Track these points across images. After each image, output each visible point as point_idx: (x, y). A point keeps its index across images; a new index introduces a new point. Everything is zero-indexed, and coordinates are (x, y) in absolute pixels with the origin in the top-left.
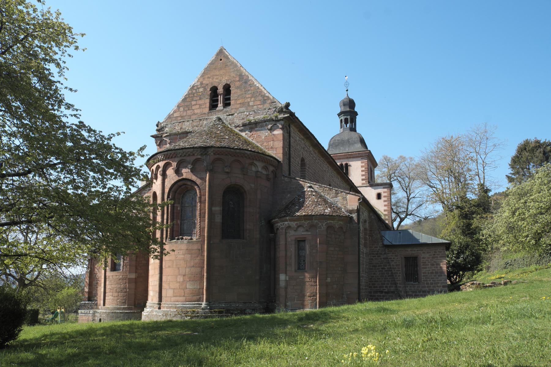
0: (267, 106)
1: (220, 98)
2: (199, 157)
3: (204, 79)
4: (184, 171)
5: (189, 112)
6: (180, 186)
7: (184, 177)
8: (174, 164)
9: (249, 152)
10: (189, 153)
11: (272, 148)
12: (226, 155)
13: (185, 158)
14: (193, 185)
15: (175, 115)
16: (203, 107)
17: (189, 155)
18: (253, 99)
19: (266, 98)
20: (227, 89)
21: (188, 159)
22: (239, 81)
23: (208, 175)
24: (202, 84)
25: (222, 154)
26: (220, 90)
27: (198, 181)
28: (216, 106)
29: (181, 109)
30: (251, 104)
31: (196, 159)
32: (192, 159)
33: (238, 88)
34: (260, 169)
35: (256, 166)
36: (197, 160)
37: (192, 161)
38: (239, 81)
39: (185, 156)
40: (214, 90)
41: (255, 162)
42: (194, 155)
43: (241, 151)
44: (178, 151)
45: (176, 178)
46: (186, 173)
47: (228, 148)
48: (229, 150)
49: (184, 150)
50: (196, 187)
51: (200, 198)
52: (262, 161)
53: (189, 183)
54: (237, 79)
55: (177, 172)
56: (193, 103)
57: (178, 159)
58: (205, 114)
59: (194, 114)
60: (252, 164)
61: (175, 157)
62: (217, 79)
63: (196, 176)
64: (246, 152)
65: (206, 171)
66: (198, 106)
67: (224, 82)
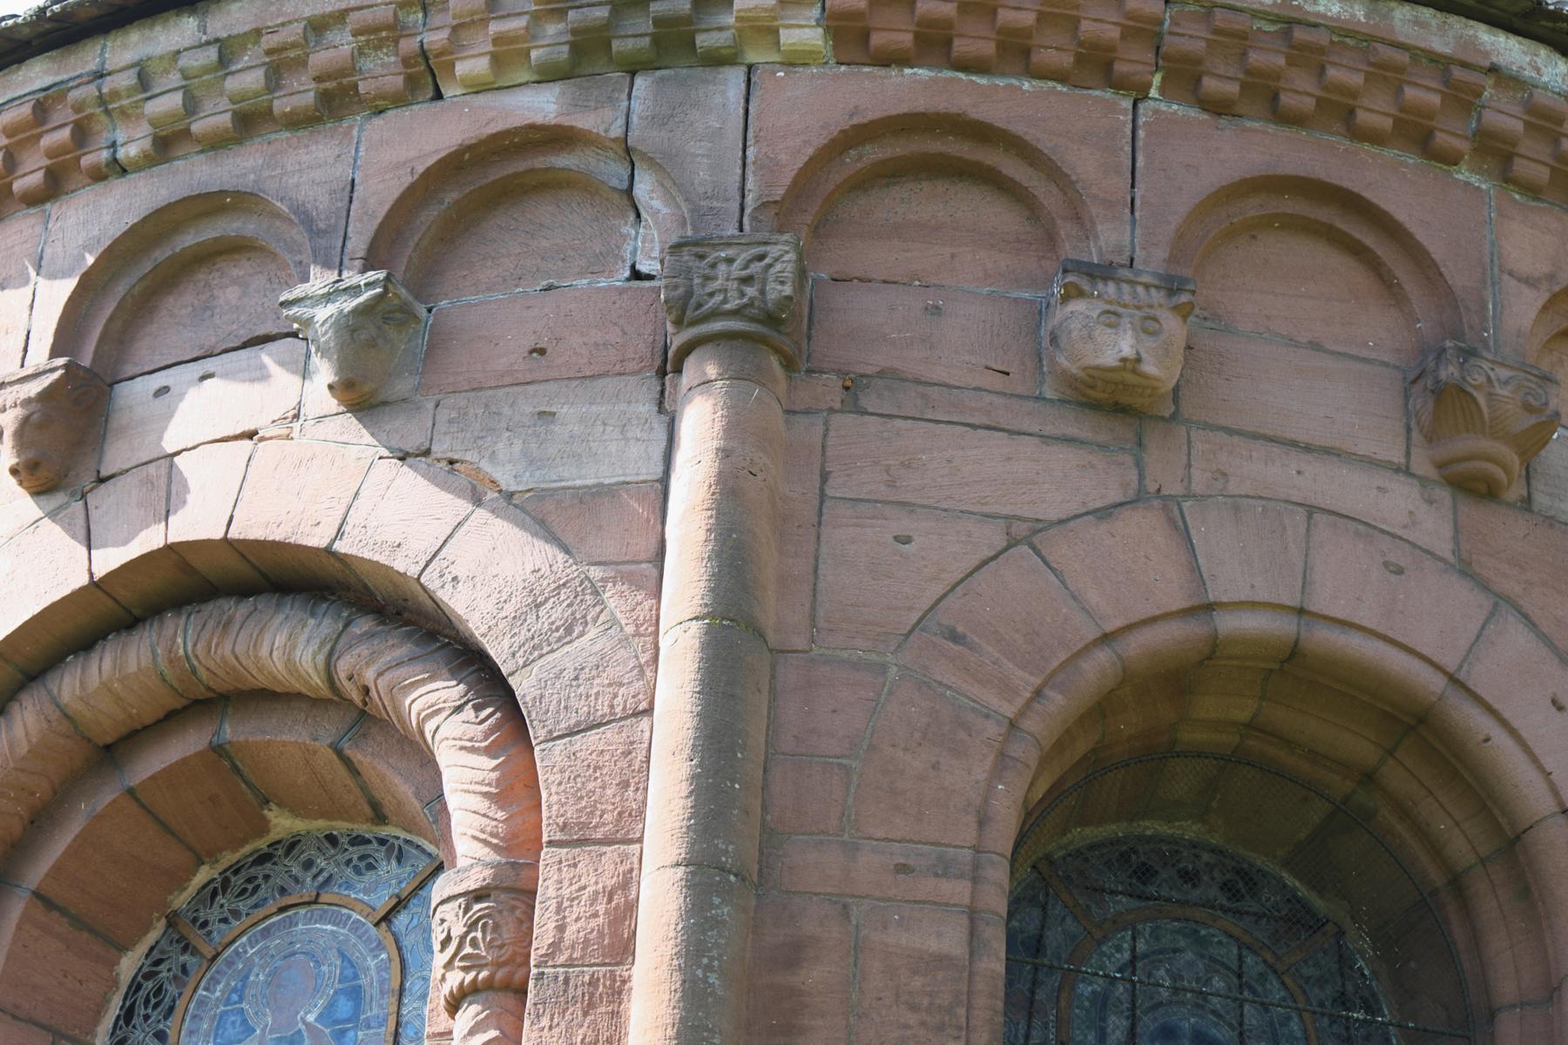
2: (542, 105)
6: (111, 752)
10: (342, 44)
17: (338, 101)
21: (304, 170)
23: (701, 422)
31: (454, 166)
32: (391, 152)
36: (490, 184)
37: (379, 193)
39: (250, 122)
42: (425, 79)
53: (288, 645)
57: (90, 222)
61: (54, 187)
65: (668, 366)
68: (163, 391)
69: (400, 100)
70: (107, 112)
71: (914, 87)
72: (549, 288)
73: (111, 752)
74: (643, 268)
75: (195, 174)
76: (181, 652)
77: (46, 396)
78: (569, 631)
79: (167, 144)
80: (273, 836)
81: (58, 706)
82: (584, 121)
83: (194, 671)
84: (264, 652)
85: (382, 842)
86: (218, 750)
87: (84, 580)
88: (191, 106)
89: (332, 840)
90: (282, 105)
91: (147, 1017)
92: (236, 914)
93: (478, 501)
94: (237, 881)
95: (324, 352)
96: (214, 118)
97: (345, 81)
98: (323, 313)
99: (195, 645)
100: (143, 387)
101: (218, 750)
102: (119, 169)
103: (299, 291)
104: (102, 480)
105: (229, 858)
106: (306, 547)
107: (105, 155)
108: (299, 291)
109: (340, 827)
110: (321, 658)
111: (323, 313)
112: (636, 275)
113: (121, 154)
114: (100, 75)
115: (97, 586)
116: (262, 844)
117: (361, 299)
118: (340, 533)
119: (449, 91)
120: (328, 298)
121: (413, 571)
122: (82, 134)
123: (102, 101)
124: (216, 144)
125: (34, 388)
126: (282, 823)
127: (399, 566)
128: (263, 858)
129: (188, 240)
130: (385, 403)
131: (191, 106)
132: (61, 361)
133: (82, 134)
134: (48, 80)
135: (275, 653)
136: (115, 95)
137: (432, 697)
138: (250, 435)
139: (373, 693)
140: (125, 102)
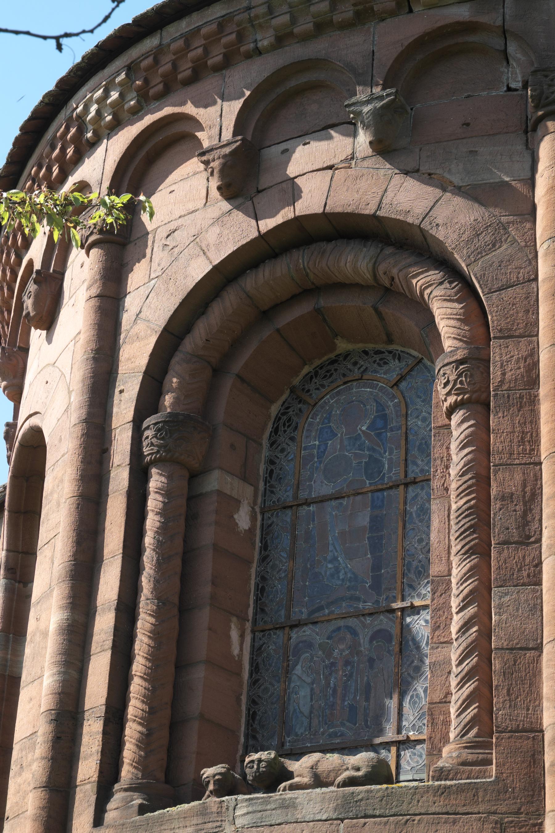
4: (307, 160)
6: (266, 314)
7: (311, 200)
8: (217, 120)
13: (317, 48)
14: (392, 265)
21: (351, 47)
27: (451, 219)
31: (420, 43)
32: (392, 36)
37: (387, 55)
39: (321, 27)
45: (231, 231)
46: (330, 171)
50: (427, 283)
51: (476, 360)
53: (354, 261)
55: (245, 176)
57: (247, 76)
61: (227, 63)
63: (428, 178)
68: (286, 151)
70: (253, 26)
72: (468, 96)
73: (266, 314)
74: (513, 85)
75: (295, 52)
76: (302, 266)
77: (232, 153)
78: (494, 245)
79: (281, 40)
80: (337, 352)
81: (245, 292)
82: (484, 19)
83: (307, 275)
84: (342, 264)
85: (390, 352)
86: (318, 311)
87: (256, 234)
88: (294, 21)
89: (366, 353)
90: (337, 18)
91: (285, 431)
92: (323, 386)
93: (444, 190)
94: (322, 372)
95: (366, 127)
96: (305, 25)
97: (367, 5)
98: (366, 109)
99: (308, 263)
100: (276, 150)
101: (318, 311)
102: (258, 52)
103: (353, 100)
104: (259, 192)
105: (317, 362)
106: (363, 215)
107: (252, 45)
108: (353, 100)
109: (370, 346)
110: (370, 265)
111: (366, 109)
112: (509, 89)
113: (260, 45)
114: (249, 8)
115: (262, 237)
116: (332, 356)
117: (384, 102)
118: (379, 207)
119: (416, 9)
120: (368, 102)
121: (417, 222)
122: (241, 37)
123: (250, 20)
124: (305, 38)
125: (227, 150)
126: (342, 346)
127: (410, 220)
128: (333, 362)
129: (293, 83)
130: (395, 150)
131: (294, 21)
132: (239, 138)
133: (241, 37)
134: (224, 12)
135: (348, 264)
136: (257, 17)
137: (428, 279)
138: (330, 167)
139: (397, 280)
140: (261, 20)
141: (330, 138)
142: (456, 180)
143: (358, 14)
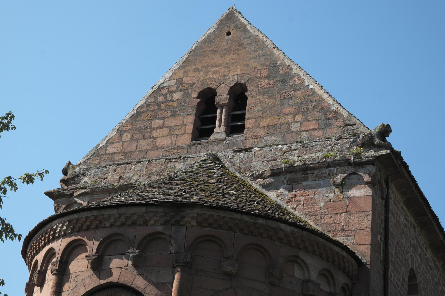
0: (333, 132)
1: (221, 115)
2: (160, 229)
3: (186, 73)
5: (144, 144)
7: (114, 278)
8: (92, 246)
9: (289, 229)
10: (135, 217)
11: (343, 230)
12: (231, 229)
13: (121, 230)
15: (110, 149)
16: (177, 132)
17: (134, 224)
18: (299, 117)
19: (330, 115)
20: (239, 95)
21: (130, 232)
22: (268, 77)
23: (177, 276)
24: (180, 82)
25: (220, 227)
26: (223, 96)
28: (211, 132)
29: (127, 136)
30: (295, 127)
32: (140, 232)
33: (263, 92)
34: (314, 276)
35: (303, 265)
36: (153, 237)
38: (268, 77)
39: (123, 224)
40: (208, 98)
41: (302, 255)
42: (146, 223)
43: (270, 223)
44: (107, 212)
45: (93, 282)
46: (120, 269)
47: (235, 211)
48: (238, 216)
49: (122, 210)
52: (321, 255)
54: (265, 73)
55: (98, 265)
56: (156, 123)
58: (180, 148)
59: (156, 148)
60: (294, 260)
61: (97, 227)
62: (216, 72)
63: (146, 278)
64: (283, 226)
65: (174, 267)
66: (165, 131)
67: (233, 78)
68: (110, 259)
69: (142, 225)
71: (207, 231)
74: (172, 252)
75: (114, 230)
77: (95, 259)
79: (112, 225)
82: (166, 232)
88: (115, 221)
90: (127, 223)
93: (149, 282)
95: (131, 260)
96: (118, 223)
98: (131, 255)
100: (107, 258)
102: (105, 227)
103: (128, 251)
104: (102, 270)
107: (104, 225)
108: (128, 251)
111: (131, 255)
112: (171, 253)
114: (103, 215)
118: (132, 284)
119: (148, 225)
120: (132, 253)
121: (141, 291)
122: (101, 222)
123: (104, 218)
124: (118, 226)
125: (94, 258)
127: (139, 290)
129: (114, 238)
131: (115, 221)
132: (97, 254)
133: (101, 222)
134: (97, 214)
138: (121, 268)
141: (122, 259)
142: (153, 280)
143: (133, 223)
